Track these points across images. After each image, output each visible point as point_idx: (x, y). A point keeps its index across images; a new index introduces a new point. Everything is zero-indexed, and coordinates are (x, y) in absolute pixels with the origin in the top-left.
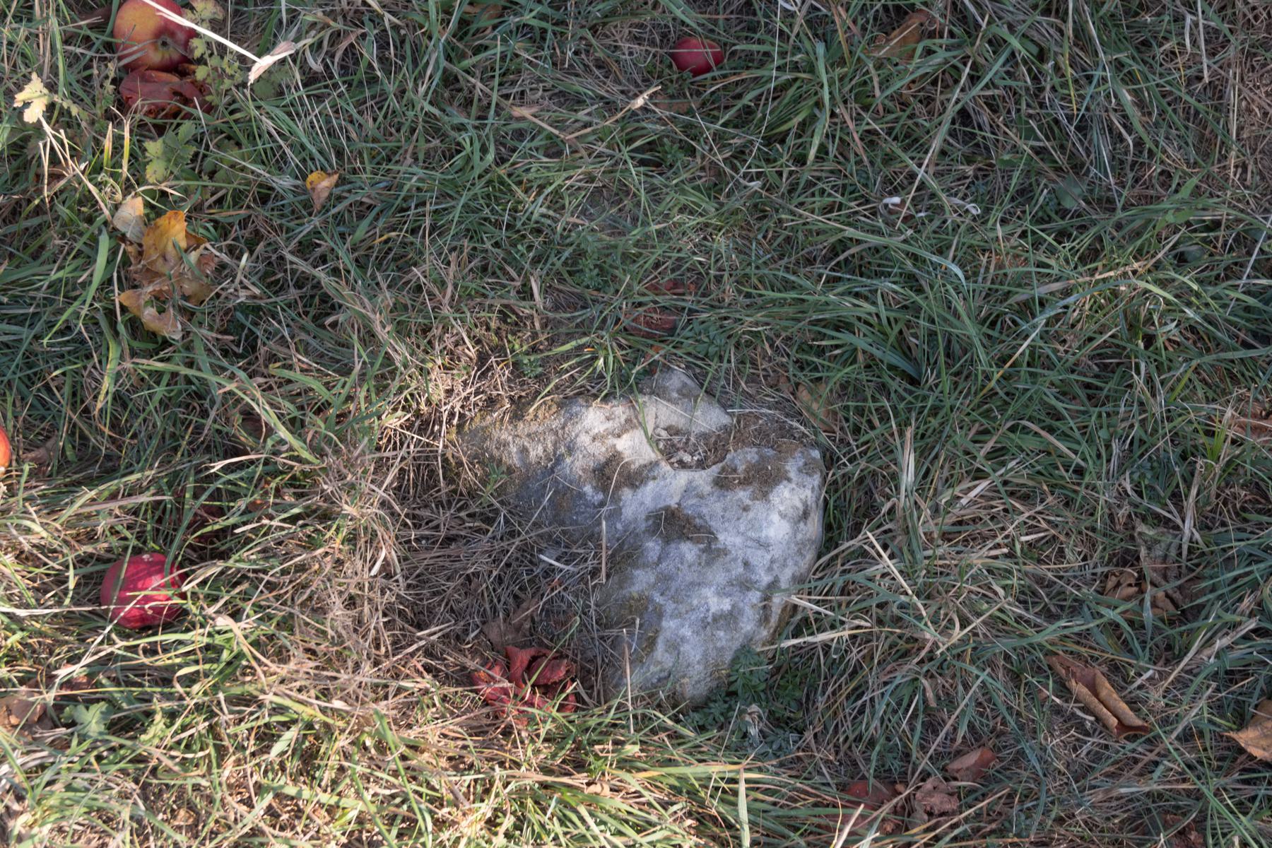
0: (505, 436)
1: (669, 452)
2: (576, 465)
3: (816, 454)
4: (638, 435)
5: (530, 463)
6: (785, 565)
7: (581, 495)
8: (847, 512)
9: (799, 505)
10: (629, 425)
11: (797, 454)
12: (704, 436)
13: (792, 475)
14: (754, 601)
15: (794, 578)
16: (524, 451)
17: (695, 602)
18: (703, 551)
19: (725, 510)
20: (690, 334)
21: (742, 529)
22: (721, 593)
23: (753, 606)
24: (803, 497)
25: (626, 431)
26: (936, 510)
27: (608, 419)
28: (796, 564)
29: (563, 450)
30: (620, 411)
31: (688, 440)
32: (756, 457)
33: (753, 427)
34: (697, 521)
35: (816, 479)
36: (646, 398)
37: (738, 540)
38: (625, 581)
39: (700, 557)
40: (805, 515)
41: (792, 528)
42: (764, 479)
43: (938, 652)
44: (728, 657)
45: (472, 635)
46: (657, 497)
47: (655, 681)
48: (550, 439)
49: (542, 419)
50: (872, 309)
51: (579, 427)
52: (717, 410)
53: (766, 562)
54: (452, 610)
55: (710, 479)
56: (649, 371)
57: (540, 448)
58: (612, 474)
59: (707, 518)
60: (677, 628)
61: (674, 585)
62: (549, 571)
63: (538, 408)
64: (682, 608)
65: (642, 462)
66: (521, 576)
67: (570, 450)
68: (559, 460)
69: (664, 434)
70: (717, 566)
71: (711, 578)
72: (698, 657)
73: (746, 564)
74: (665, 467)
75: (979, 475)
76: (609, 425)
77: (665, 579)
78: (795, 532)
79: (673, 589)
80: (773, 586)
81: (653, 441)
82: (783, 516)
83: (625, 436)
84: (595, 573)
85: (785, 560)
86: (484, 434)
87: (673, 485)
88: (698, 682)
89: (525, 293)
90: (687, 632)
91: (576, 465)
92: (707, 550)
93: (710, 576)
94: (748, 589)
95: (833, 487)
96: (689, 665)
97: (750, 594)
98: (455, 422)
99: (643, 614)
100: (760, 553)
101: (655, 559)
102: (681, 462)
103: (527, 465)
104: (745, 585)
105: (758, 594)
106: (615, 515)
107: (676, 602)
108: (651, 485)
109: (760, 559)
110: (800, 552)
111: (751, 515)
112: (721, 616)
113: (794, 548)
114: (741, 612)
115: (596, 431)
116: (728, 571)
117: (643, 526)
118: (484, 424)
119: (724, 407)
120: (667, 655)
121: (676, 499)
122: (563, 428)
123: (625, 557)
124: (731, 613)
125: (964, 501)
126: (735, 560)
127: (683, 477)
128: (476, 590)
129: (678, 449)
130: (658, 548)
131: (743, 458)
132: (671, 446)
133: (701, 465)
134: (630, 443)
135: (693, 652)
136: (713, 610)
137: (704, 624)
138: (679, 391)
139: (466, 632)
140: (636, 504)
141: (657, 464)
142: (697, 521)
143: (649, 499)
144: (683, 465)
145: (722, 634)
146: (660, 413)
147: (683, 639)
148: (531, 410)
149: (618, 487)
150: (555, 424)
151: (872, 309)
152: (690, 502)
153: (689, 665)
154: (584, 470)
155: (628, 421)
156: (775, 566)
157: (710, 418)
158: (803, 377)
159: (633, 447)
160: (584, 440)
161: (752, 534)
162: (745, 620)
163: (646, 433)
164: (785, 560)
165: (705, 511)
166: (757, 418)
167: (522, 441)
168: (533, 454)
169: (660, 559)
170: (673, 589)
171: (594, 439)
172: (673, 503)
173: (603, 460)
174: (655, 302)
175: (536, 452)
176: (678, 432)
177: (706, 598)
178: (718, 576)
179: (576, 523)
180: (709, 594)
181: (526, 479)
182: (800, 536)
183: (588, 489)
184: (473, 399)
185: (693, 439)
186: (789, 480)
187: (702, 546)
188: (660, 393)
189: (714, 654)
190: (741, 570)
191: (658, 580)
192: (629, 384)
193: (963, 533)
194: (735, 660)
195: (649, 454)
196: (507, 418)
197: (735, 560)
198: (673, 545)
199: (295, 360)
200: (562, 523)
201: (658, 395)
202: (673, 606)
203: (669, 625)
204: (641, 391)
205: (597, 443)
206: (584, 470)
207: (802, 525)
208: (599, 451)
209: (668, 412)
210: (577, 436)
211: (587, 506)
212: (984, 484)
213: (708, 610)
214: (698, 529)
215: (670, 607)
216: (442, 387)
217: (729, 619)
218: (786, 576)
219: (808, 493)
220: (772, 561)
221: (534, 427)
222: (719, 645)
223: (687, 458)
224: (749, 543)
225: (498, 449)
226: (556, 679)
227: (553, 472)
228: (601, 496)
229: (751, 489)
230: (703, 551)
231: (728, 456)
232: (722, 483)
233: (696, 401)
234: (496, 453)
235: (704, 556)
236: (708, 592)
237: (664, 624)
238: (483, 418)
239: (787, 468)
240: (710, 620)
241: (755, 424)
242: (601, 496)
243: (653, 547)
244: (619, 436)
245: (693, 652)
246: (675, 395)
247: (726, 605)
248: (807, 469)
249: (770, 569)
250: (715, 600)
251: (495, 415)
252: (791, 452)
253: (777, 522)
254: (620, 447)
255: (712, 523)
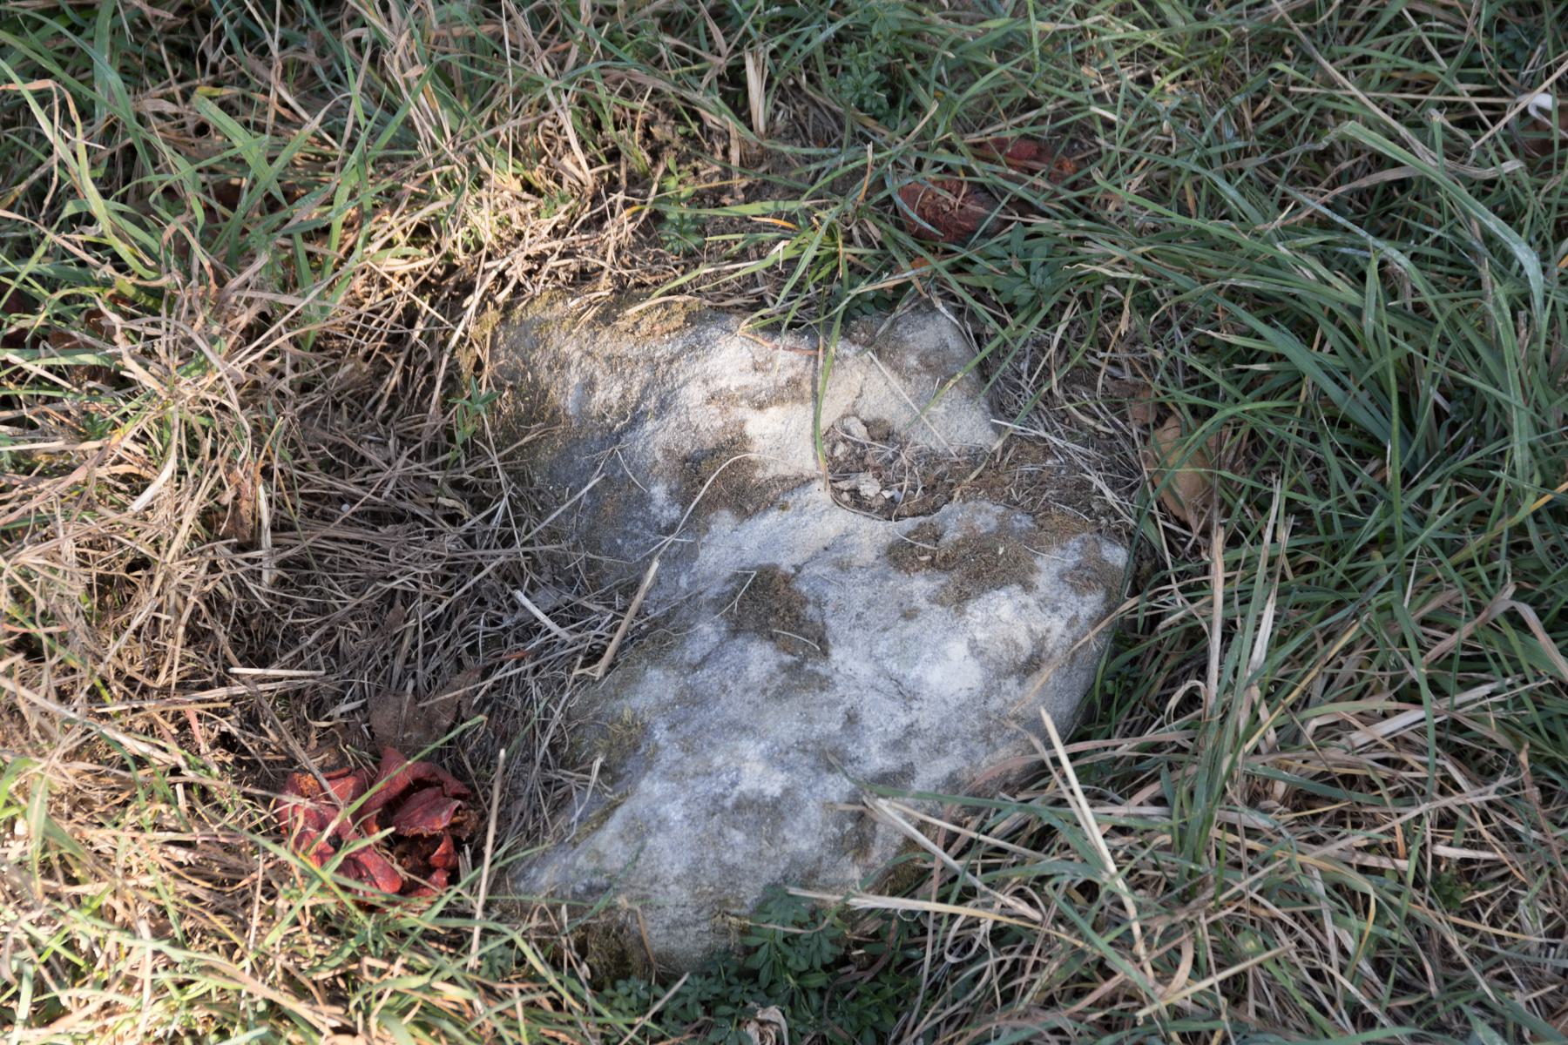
0: (571, 349)
1: (840, 471)
2: (657, 439)
3: (1117, 556)
4: (800, 416)
5: (588, 413)
6: (939, 750)
7: (644, 500)
8: (1133, 685)
9: (1027, 645)
10: (790, 392)
11: (1074, 543)
12: (930, 458)
13: (1043, 580)
14: (834, 796)
15: (953, 783)
16: (590, 385)
17: (718, 760)
18: (784, 668)
19: (869, 604)
20: (998, 252)
21: (881, 649)
22: (776, 759)
23: (828, 806)
24: (1039, 628)
25: (780, 401)
26: (1289, 738)
27: (756, 368)
28: (969, 756)
29: (652, 403)
30: (787, 357)
31: (897, 455)
32: (994, 523)
33: (1028, 468)
34: (810, 610)
35: (1091, 603)
36: (850, 351)
37: (865, 670)
38: (630, 682)
39: (772, 677)
40: (1030, 666)
41: (987, 682)
42: (978, 569)
43: (1141, 1014)
44: (750, 893)
45: (344, 707)
46: (772, 543)
47: (581, 888)
48: (643, 375)
49: (647, 329)
50: (1351, 296)
51: (698, 367)
52: (978, 415)
53: (894, 729)
54: (336, 651)
55: (885, 541)
56: (886, 302)
57: (617, 389)
58: (722, 480)
59: (829, 609)
60: (662, 800)
61: (700, 716)
62: (530, 629)
63: (648, 311)
64: (691, 764)
65: (782, 470)
66: (476, 626)
67: (664, 407)
68: (637, 421)
69: (859, 432)
70: (795, 703)
71: (769, 723)
72: (678, 870)
73: (852, 719)
74: (819, 493)
75: (1410, 695)
76: (754, 380)
77: (692, 699)
78: (989, 692)
79: (695, 724)
80: (892, 782)
81: (824, 438)
82: (975, 650)
83: (773, 411)
84: (593, 657)
85: (944, 739)
86: (536, 334)
87: (813, 529)
88: (679, 924)
89: (733, 86)
90: (675, 812)
91: (657, 439)
92: (794, 670)
93: (769, 720)
94: (830, 768)
95: (1125, 636)
96: (654, 880)
97: (831, 778)
98: (502, 297)
99: (627, 755)
100: (890, 706)
101: (698, 657)
102: (855, 492)
103: (584, 415)
104: (830, 758)
105: (848, 786)
106: (686, 555)
107: (688, 749)
108: (773, 516)
109: (882, 718)
110: (985, 736)
111: (913, 628)
112: (751, 803)
113: (974, 722)
114: (797, 808)
115: (723, 384)
116: (810, 721)
117: (712, 592)
118: (547, 315)
119: (999, 408)
120: (619, 845)
121: (798, 558)
122: (671, 362)
123: (656, 637)
124: (776, 803)
125: (1360, 738)
126: (833, 704)
127: (842, 520)
128: (391, 627)
129: (866, 468)
130: (714, 639)
131: (968, 517)
132: (853, 460)
133: (889, 510)
134: (779, 428)
135: (670, 856)
136: (744, 786)
137: (715, 806)
138: (923, 357)
139: (337, 698)
140: (731, 546)
141: (804, 482)
142: (810, 610)
143: (754, 544)
144: (858, 501)
145: (738, 837)
146: (864, 386)
147: (662, 824)
148: (632, 311)
149: (710, 504)
150: (662, 351)
151: (1351, 296)
152: (817, 570)
153: (654, 880)
154: (668, 452)
155: (794, 383)
156: (914, 745)
157: (957, 425)
158: (1183, 397)
159: (780, 438)
160: (693, 394)
161: (892, 666)
162: (800, 826)
163: (816, 420)
164: (944, 739)
165: (832, 594)
166: (1048, 452)
167: (590, 364)
168: (599, 396)
169: (705, 659)
170: (695, 724)
171: (711, 399)
172: (786, 563)
173: (710, 443)
174: (968, 171)
175: (609, 393)
176: (888, 436)
177: (743, 759)
178: (785, 724)
179: (615, 551)
180: (750, 755)
181: (574, 442)
182: (996, 703)
183: (659, 492)
184: (553, 262)
185: (904, 459)
186: (1028, 587)
187: (788, 659)
188: (883, 348)
189: (715, 873)
190: (835, 727)
191: (681, 698)
192: (827, 309)
193: (1325, 802)
194: (761, 909)
195: (805, 459)
196: (589, 315)
197: (833, 704)
198: (740, 641)
199: (273, 97)
200: (594, 546)
201: (879, 352)
202: (680, 755)
203: (652, 787)
204: (846, 334)
205: (713, 409)
206: (668, 452)
207: (1011, 684)
208: (709, 422)
209: (885, 391)
210: (685, 383)
211: (647, 526)
212: (1414, 714)
213: (734, 784)
214: (798, 623)
215: (670, 754)
216: (493, 213)
217: (767, 814)
218: (931, 773)
219: (1058, 625)
220: (910, 731)
221: (626, 347)
222: (727, 857)
223: (869, 487)
224: (882, 683)
225: (550, 369)
226: (424, 830)
227: (618, 441)
228: (675, 513)
229: (943, 579)
230: (784, 668)
231: (946, 508)
232: (899, 556)
233: (943, 384)
234: (544, 376)
235: (781, 679)
236: (751, 750)
237: (644, 784)
238: (550, 304)
239: (1039, 563)
240: (728, 803)
241: (1035, 462)
242: (675, 513)
243: (708, 631)
244: (761, 407)
245: (670, 856)
246: (912, 361)
247: (774, 786)
248: (1080, 579)
249: (897, 745)
250: (759, 768)
251: (573, 303)
252: (1062, 534)
253: (962, 664)
254: (750, 430)
255: (831, 622)
